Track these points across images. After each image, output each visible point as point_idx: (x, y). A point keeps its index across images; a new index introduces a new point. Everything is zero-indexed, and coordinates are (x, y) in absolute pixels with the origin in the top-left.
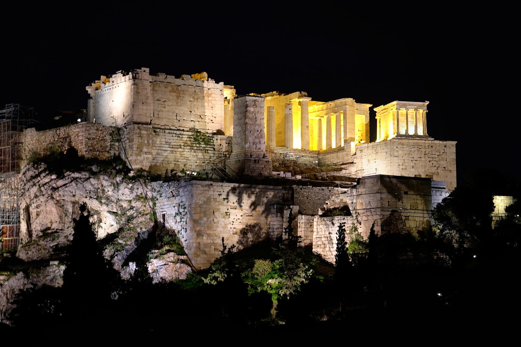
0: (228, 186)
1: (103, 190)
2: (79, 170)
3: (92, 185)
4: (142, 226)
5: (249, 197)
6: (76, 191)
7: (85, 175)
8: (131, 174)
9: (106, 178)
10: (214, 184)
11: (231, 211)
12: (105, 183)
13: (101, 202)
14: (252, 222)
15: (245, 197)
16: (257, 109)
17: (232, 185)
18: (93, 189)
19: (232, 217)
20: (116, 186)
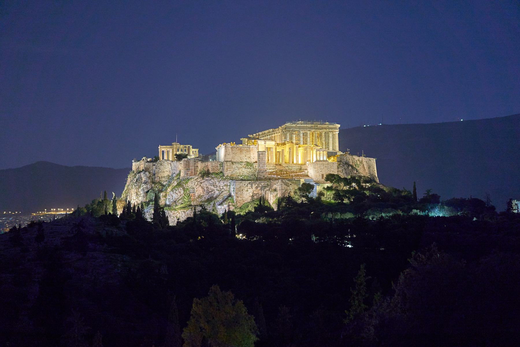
0: (247, 182)
4: (225, 194)
6: (207, 183)
15: (253, 185)
20: (219, 182)
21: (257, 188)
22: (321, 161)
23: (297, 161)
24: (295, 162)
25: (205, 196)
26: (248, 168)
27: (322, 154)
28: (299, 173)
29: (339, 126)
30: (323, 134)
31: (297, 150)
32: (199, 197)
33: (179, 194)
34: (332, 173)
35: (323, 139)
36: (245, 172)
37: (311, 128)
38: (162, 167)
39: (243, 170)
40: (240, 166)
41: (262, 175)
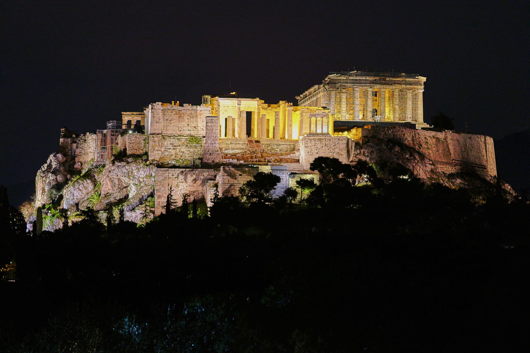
0: (178, 171)
1: (132, 172)
2: (121, 161)
3: (126, 169)
5: (192, 176)
7: (124, 164)
8: (148, 163)
9: (134, 165)
10: (170, 169)
11: (179, 184)
12: (133, 168)
13: (130, 179)
14: (194, 190)
15: (189, 176)
16: (213, 125)
17: (181, 170)
18: (126, 172)
19: (180, 187)
21: (195, 180)
22: (318, 134)
23: (290, 135)
24: (286, 137)
25: (115, 195)
26: (191, 147)
27: (319, 123)
28: (286, 157)
29: (424, 79)
30: (396, 93)
31: (290, 116)
32: (107, 195)
33: (84, 191)
34: (324, 155)
35: (397, 102)
36: (187, 153)
37: (374, 82)
38: (85, 145)
39: (183, 150)
40: (176, 143)
41: (209, 159)
